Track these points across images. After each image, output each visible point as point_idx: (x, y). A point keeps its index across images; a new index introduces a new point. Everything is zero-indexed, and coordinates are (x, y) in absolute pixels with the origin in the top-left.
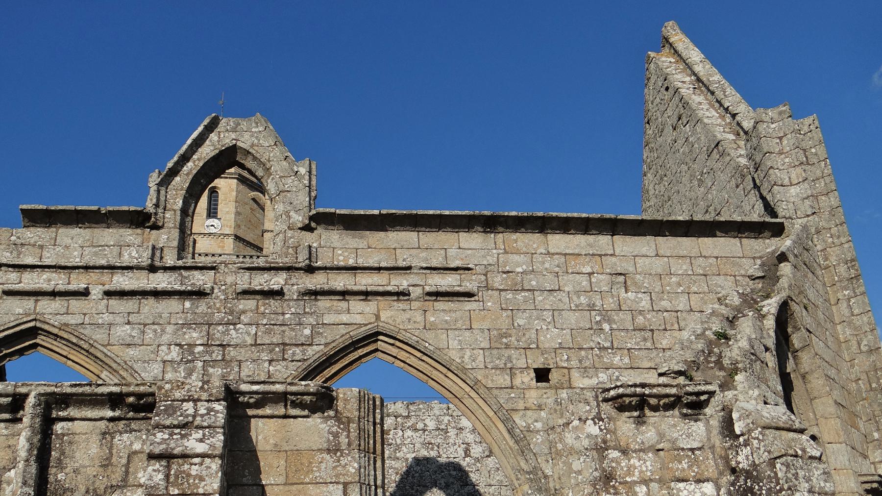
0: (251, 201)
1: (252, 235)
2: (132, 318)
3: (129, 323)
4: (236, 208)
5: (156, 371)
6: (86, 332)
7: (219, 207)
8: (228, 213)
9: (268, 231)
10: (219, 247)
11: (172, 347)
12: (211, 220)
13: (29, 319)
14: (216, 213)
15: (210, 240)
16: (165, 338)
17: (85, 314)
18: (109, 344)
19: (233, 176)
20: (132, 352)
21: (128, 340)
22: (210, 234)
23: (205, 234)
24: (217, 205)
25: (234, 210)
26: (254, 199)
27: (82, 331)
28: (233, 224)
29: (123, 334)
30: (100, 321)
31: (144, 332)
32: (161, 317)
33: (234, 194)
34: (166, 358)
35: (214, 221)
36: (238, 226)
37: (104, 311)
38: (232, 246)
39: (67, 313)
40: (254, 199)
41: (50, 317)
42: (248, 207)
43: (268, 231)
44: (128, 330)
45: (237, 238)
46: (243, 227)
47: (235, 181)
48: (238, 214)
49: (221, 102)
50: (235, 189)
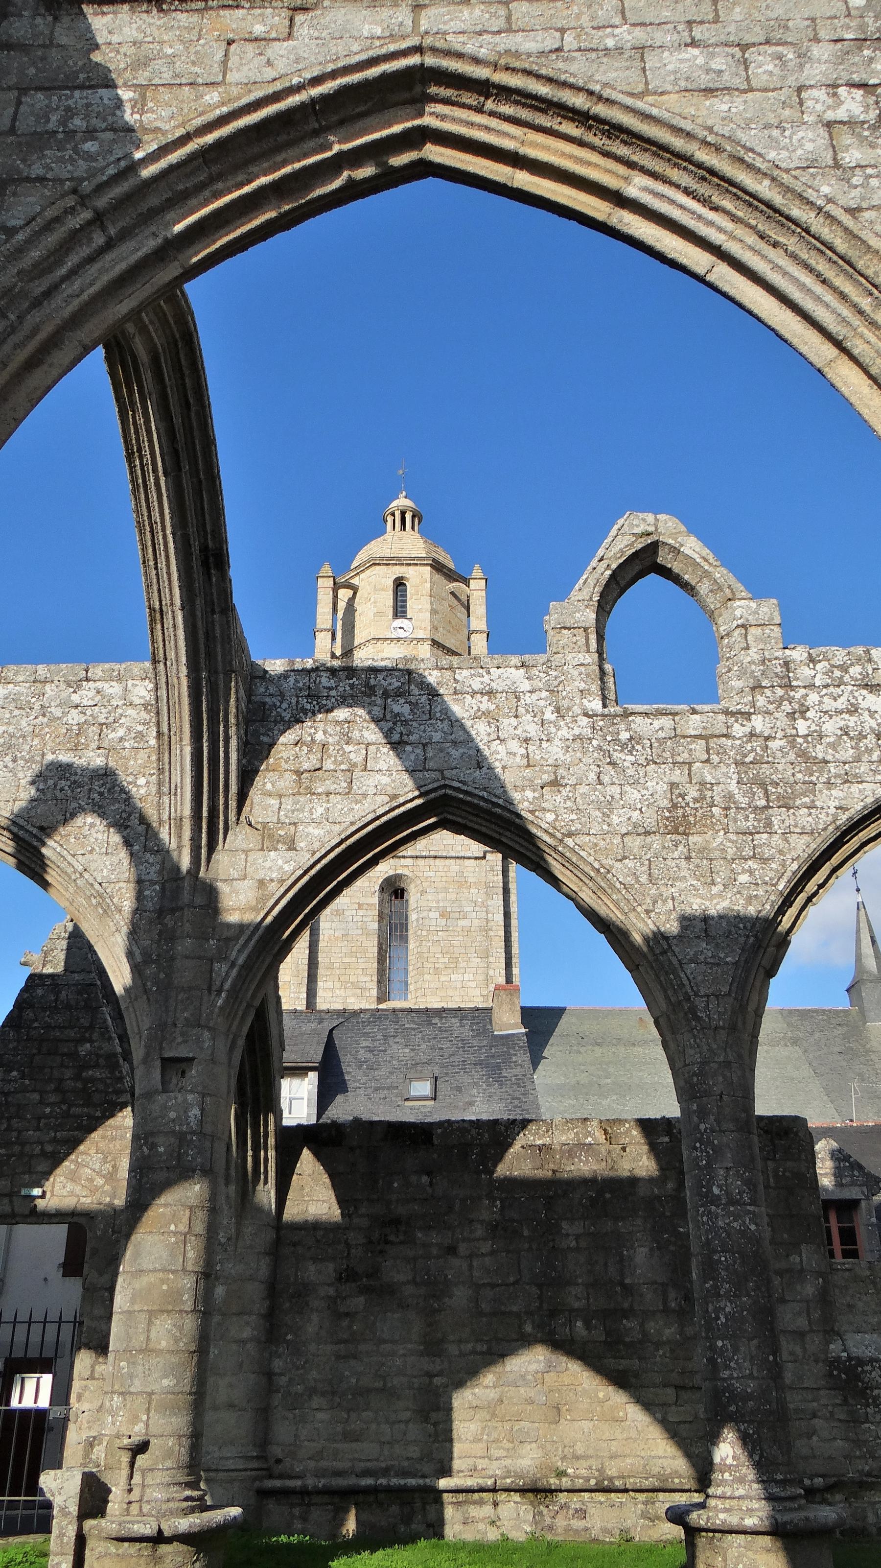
0: (450, 596)
1: (453, 641)
2: (698, 32)
3: (693, 43)
4: (432, 604)
5: (809, 146)
6: (574, 68)
8: (420, 610)
9: (477, 632)
11: (842, 91)
13: (404, 45)
14: (405, 612)
16: (814, 73)
17: (562, 31)
18: (646, 93)
20: (721, 105)
21: (705, 80)
22: (399, 639)
23: (392, 640)
24: (405, 601)
25: (428, 607)
26: (452, 593)
27: (560, 65)
28: (428, 625)
29: (684, 67)
30: (610, 43)
31: (746, 64)
32: (786, 27)
33: (428, 585)
34: (830, 115)
36: (435, 628)
37: (617, 20)
39: (510, 30)
40: (452, 593)
41: (461, 38)
43: (477, 632)
44: (696, 57)
45: (435, 643)
48: (434, 612)
49: (401, 472)
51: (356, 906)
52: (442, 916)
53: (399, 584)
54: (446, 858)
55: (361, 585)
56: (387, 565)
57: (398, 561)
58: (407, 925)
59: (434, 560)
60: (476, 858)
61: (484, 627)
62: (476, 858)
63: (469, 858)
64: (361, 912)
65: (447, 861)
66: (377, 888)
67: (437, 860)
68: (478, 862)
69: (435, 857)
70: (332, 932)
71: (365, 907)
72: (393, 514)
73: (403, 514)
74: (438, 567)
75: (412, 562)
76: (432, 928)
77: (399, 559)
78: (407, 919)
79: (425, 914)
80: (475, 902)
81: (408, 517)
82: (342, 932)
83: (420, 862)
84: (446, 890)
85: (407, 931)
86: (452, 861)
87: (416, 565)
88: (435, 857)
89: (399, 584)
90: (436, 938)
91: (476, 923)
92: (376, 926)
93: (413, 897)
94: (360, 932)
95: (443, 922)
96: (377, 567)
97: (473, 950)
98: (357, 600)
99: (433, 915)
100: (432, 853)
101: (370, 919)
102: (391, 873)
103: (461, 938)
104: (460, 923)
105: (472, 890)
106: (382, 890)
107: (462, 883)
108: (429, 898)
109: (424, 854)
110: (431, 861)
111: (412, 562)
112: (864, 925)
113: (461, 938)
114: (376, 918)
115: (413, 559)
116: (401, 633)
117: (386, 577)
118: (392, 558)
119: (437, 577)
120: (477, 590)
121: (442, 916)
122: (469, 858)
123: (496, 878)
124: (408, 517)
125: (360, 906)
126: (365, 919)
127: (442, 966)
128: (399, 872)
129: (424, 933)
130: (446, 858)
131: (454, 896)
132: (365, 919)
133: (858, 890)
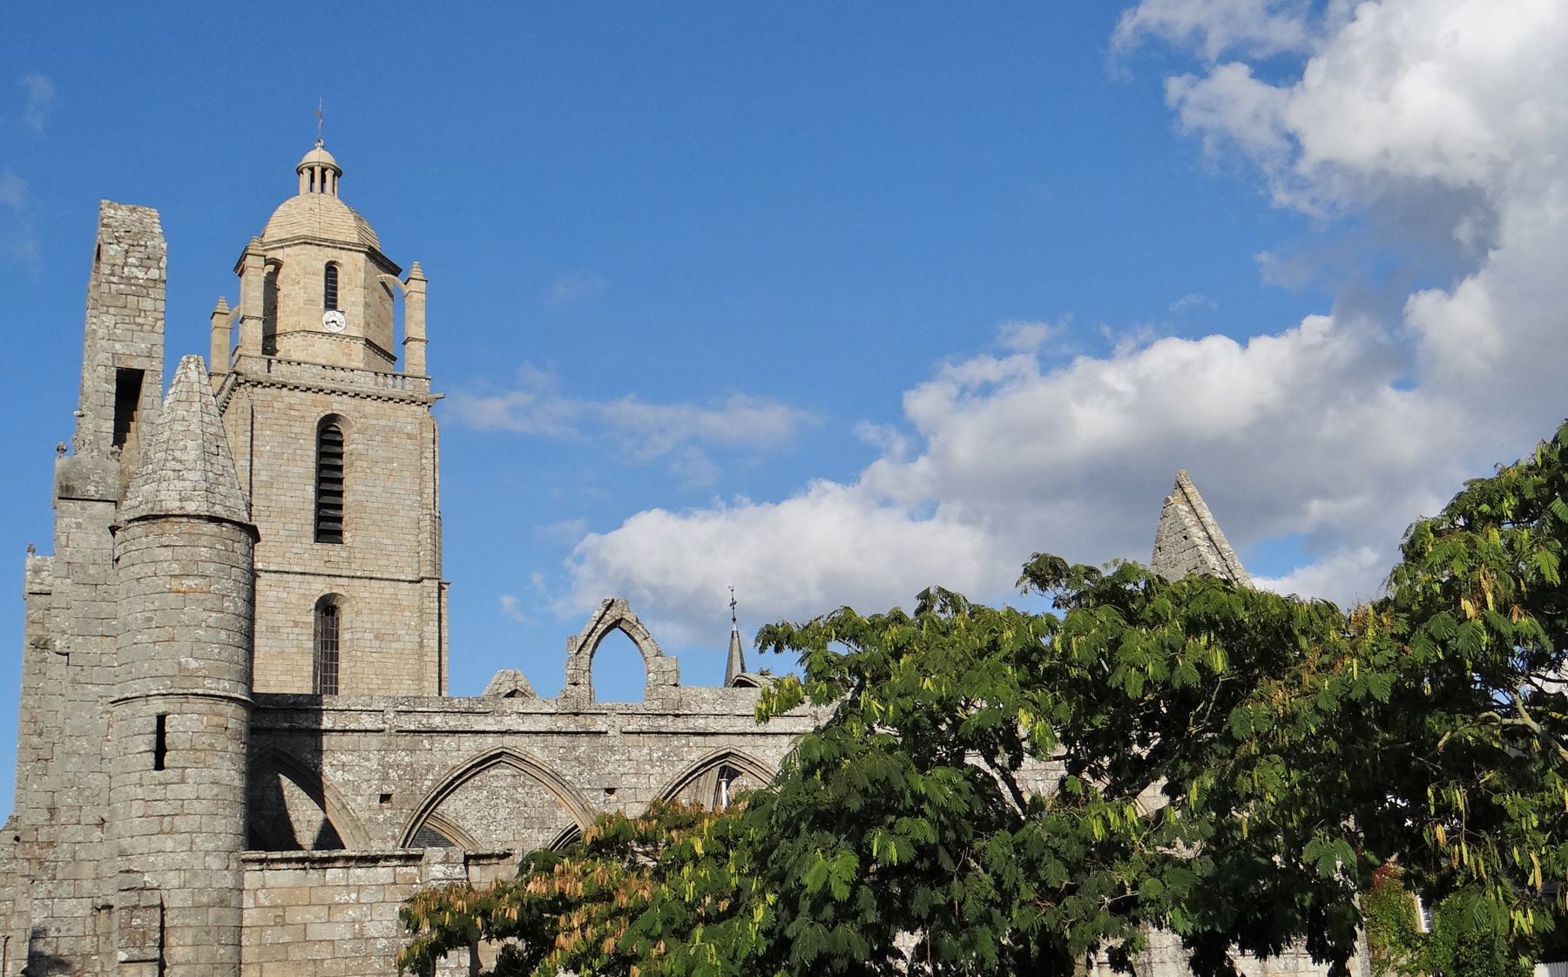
1: (382, 337)
7: (339, 294)
8: (354, 303)
10: (345, 354)
12: (331, 312)
15: (331, 344)
19: (361, 249)
22: (331, 335)
23: (324, 334)
26: (383, 284)
33: (363, 275)
35: (330, 315)
38: (362, 355)
40: (383, 284)
42: (377, 295)
45: (369, 343)
46: (372, 325)
47: (363, 255)
48: (367, 305)
50: (363, 269)
51: (292, 624)
52: (377, 637)
53: (331, 269)
54: (382, 579)
55: (286, 261)
56: (320, 245)
57: (333, 244)
58: (337, 642)
59: (371, 248)
60: (410, 582)
61: (422, 335)
62: (410, 582)
63: (404, 581)
64: (297, 630)
65: (382, 582)
66: (313, 606)
67: (373, 581)
68: (412, 585)
69: (371, 578)
70: (267, 649)
71: (301, 625)
72: (312, 169)
73: (324, 170)
74: (373, 255)
75: (345, 247)
76: (367, 649)
77: (333, 241)
78: (337, 637)
79: (359, 635)
80: (409, 625)
81: (329, 174)
82: (278, 650)
83: (356, 582)
84: (380, 612)
85: (337, 649)
86: (387, 582)
87: (351, 250)
88: (371, 578)
89: (331, 269)
90: (370, 659)
91: (409, 646)
92: (311, 644)
93: (346, 617)
94: (295, 650)
95: (377, 643)
96: (308, 246)
97: (405, 672)
98: (280, 277)
99: (368, 636)
100: (367, 574)
101: (305, 637)
102: (327, 591)
103: (394, 661)
104: (394, 645)
105: (405, 614)
106: (317, 608)
107: (396, 606)
108: (365, 619)
109: (359, 574)
110: (367, 581)
111: (345, 247)
112: (736, 653)
113: (394, 661)
114: (312, 637)
115: (348, 244)
116: (334, 329)
117: (318, 259)
118: (326, 240)
119: (371, 265)
120: (416, 292)
121: (377, 637)
122: (404, 581)
123: (432, 605)
124: (329, 174)
125: (296, 624)
126: (301, 638)
127: (374, 687)
128: (334, 591)
129: (359, 654)
130: (382, 579)
131: (387, 619)
132: (301, 638)
133: (734, 620)
